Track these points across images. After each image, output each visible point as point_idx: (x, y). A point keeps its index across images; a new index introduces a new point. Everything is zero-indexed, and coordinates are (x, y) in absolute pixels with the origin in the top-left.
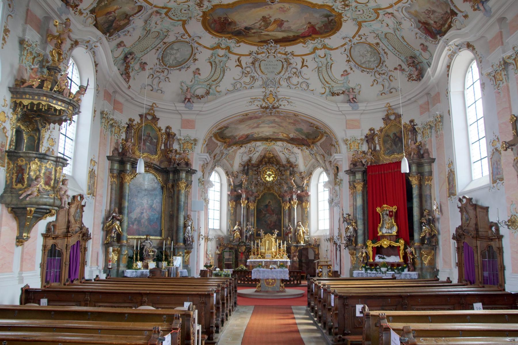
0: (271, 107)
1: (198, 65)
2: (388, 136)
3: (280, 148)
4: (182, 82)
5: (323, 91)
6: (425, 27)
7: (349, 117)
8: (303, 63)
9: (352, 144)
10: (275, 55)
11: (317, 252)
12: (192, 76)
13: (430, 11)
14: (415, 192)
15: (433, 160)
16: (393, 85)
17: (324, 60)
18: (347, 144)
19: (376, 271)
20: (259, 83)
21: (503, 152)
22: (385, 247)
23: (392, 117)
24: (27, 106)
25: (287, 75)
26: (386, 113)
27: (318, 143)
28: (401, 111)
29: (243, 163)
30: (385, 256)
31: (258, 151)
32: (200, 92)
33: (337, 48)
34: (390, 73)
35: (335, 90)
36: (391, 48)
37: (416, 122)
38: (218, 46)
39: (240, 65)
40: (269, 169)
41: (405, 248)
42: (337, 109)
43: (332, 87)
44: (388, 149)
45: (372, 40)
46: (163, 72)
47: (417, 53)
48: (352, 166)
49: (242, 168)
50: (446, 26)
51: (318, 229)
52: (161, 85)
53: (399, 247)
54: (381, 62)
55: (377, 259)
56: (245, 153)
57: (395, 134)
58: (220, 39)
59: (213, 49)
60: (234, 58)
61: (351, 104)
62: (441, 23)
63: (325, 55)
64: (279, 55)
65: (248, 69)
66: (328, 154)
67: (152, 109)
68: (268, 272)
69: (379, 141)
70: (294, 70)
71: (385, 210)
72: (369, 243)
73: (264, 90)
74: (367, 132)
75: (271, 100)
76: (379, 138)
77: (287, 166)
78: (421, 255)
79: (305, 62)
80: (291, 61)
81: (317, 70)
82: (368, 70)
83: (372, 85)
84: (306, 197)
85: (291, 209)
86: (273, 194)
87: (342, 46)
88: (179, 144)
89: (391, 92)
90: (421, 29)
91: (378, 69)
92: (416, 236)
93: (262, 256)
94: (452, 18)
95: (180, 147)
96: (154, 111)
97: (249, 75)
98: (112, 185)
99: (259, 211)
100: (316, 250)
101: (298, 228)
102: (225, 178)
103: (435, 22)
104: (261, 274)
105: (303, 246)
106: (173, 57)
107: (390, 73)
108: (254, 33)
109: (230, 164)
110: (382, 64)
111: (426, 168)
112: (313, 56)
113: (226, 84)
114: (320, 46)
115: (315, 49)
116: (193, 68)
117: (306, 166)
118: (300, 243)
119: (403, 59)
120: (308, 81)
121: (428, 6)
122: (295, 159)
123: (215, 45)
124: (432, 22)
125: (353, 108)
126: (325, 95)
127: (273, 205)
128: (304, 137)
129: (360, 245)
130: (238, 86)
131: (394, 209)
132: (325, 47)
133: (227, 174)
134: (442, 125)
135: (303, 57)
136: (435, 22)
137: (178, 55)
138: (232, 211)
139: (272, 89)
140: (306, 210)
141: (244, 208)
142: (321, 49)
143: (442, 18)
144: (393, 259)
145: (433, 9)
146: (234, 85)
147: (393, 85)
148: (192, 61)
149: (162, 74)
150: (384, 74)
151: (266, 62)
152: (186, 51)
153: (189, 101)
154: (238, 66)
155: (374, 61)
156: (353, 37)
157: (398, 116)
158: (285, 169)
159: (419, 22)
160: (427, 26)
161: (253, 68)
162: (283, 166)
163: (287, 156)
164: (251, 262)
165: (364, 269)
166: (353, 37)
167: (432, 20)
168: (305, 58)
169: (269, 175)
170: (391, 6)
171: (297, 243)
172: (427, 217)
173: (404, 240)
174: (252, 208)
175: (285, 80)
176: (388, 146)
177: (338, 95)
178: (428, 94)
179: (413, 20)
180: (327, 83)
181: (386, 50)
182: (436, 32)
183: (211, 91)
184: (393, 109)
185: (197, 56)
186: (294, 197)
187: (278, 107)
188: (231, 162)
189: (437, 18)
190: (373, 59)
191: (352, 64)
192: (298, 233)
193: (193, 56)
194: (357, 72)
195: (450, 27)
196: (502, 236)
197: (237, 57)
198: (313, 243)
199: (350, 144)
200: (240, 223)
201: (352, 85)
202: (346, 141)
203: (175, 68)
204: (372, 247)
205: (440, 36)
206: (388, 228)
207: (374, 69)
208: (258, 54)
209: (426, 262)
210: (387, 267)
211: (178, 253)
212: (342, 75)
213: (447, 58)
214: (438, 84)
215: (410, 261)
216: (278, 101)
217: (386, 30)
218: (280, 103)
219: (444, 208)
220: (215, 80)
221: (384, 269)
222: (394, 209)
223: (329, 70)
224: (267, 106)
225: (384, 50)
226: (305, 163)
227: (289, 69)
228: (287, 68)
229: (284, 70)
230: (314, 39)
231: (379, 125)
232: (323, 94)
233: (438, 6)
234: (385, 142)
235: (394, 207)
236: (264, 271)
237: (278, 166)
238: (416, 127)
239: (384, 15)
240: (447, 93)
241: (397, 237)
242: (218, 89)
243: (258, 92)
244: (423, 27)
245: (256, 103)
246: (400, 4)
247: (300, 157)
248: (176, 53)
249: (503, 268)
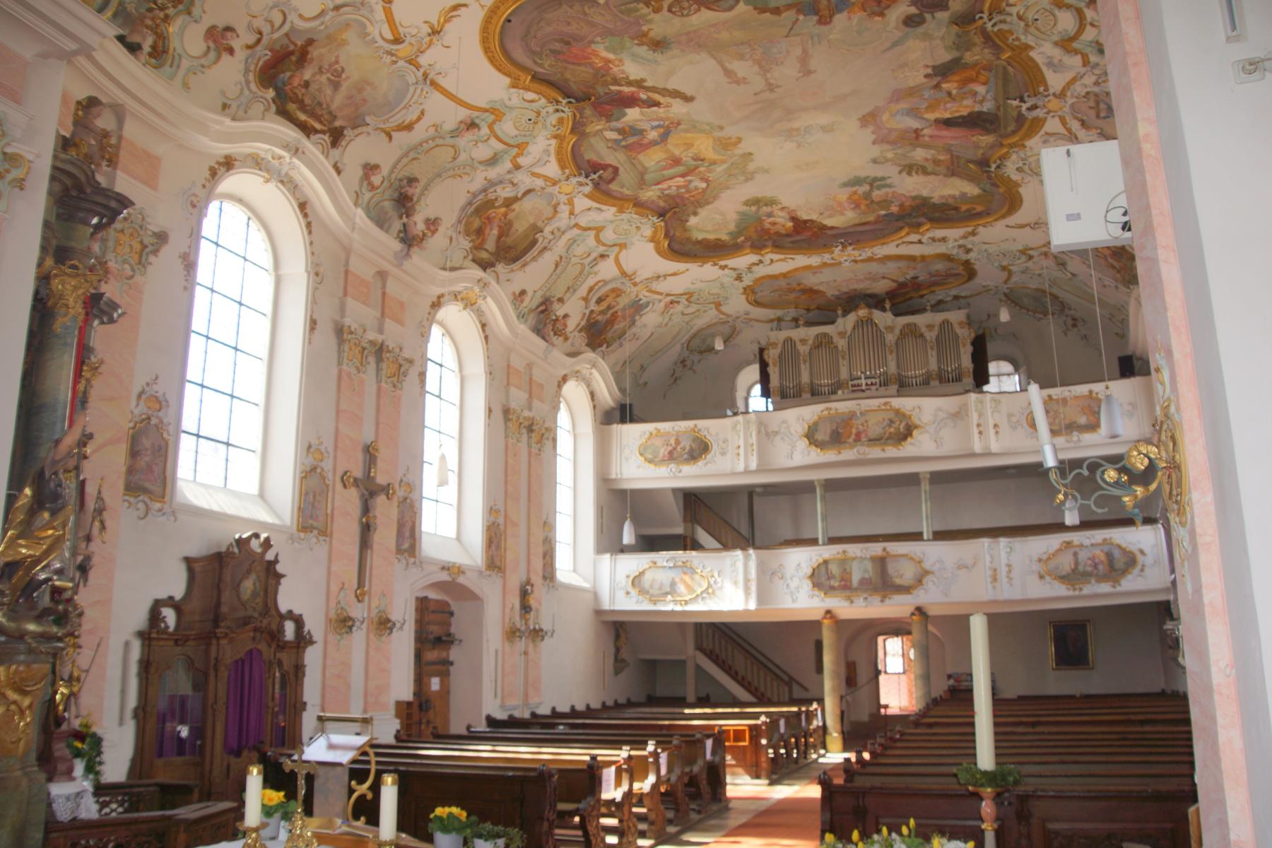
6: (292, 53)
13: (339, 76)
62: (307, 101)
90: (286, 41)
94: (323, 132)
103: (307, 84)
121: (353, 74)
124: (307, 76)
143: (320, 104)
145: (345, 86)
159: (310, 42)
167: (314, 75)
182: (280, 85)
189: (319, 90)
195: (307, 130)
233: (350, 97)
244: (292, 47)
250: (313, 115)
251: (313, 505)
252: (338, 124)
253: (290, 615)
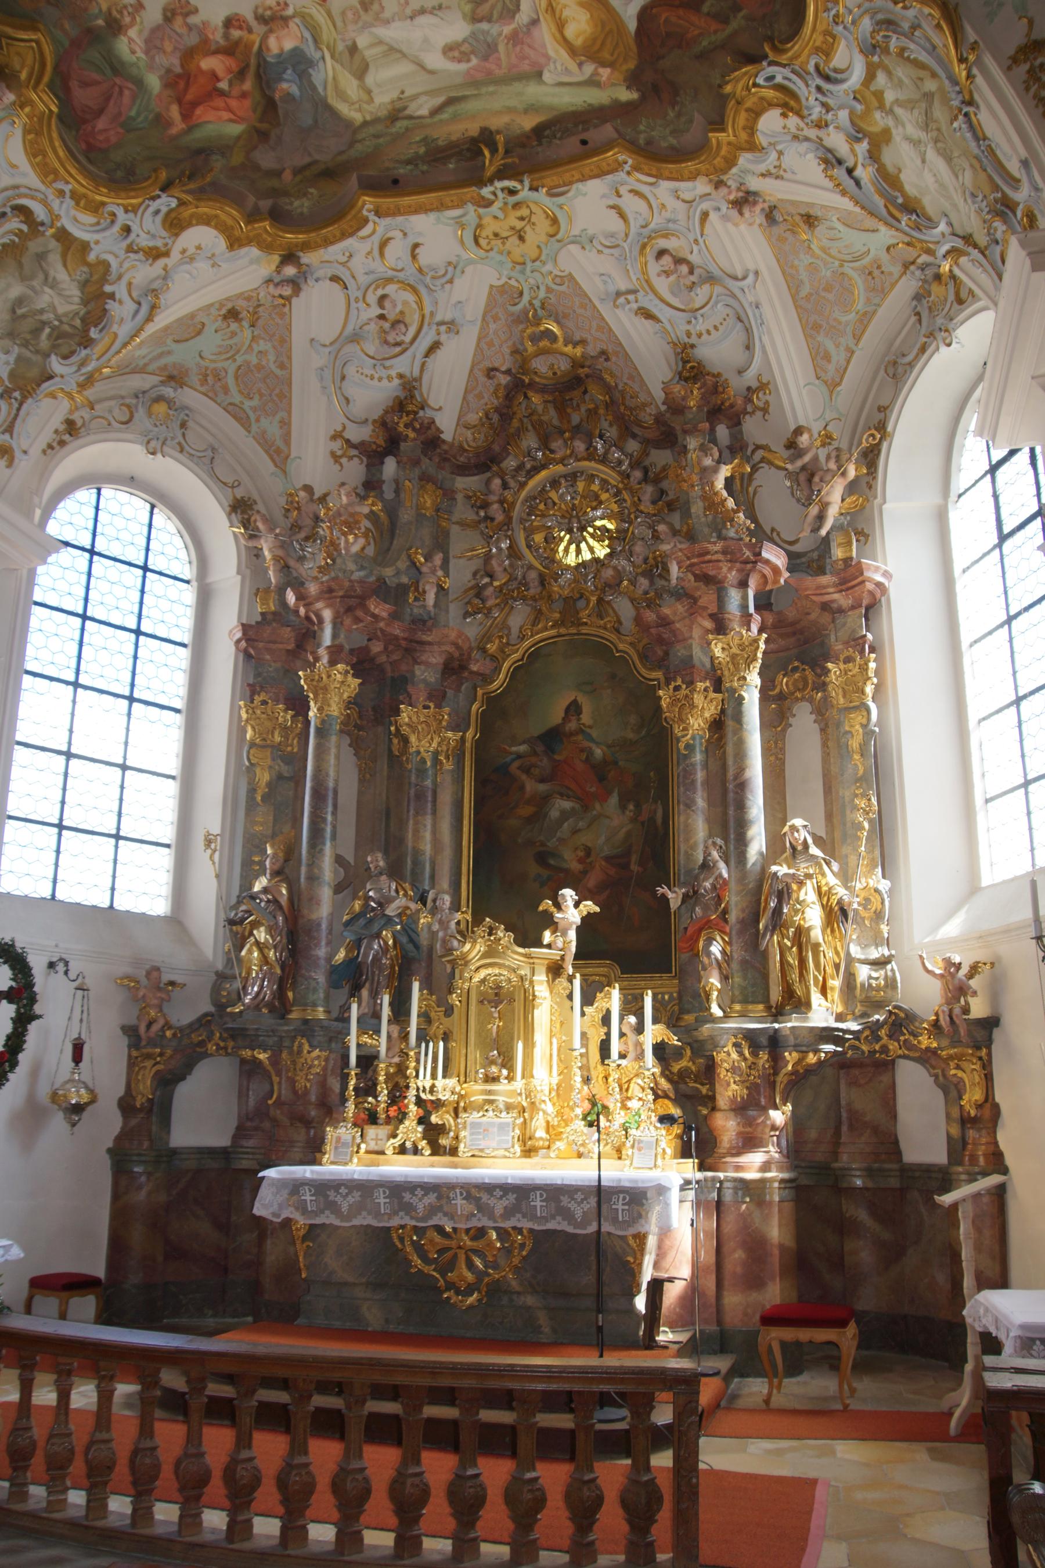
3: (606, 264)
11: (973, 1095)
29: (357, 434)
31: (452, 326)
49: (355, 470)
51: (973, 888)
56: (355, 338)
84: (855, 620)
85: (724, 726)
86: (601, 651)
93: (433, 1133)
99: (493, 783)
100: (969, 1075)
101: (781, 870)
102: (225, 538)
105: (827, 1035)
109: (264, 442)
117: (832, 386)
118: (803, 1005)
122: (737, 335)
127: (601, 725)
133: (241, 509)
138: (264, 777)
140: (854, 723)
141: (321, 732)
163: (679, 326)
164: (296, 1186)
171: (777, 1013)
174: (424, 745)
188: (272, 427)
192: (777, 921)
198: (924, 996)
200: (290, 853)
226: (819, 357)
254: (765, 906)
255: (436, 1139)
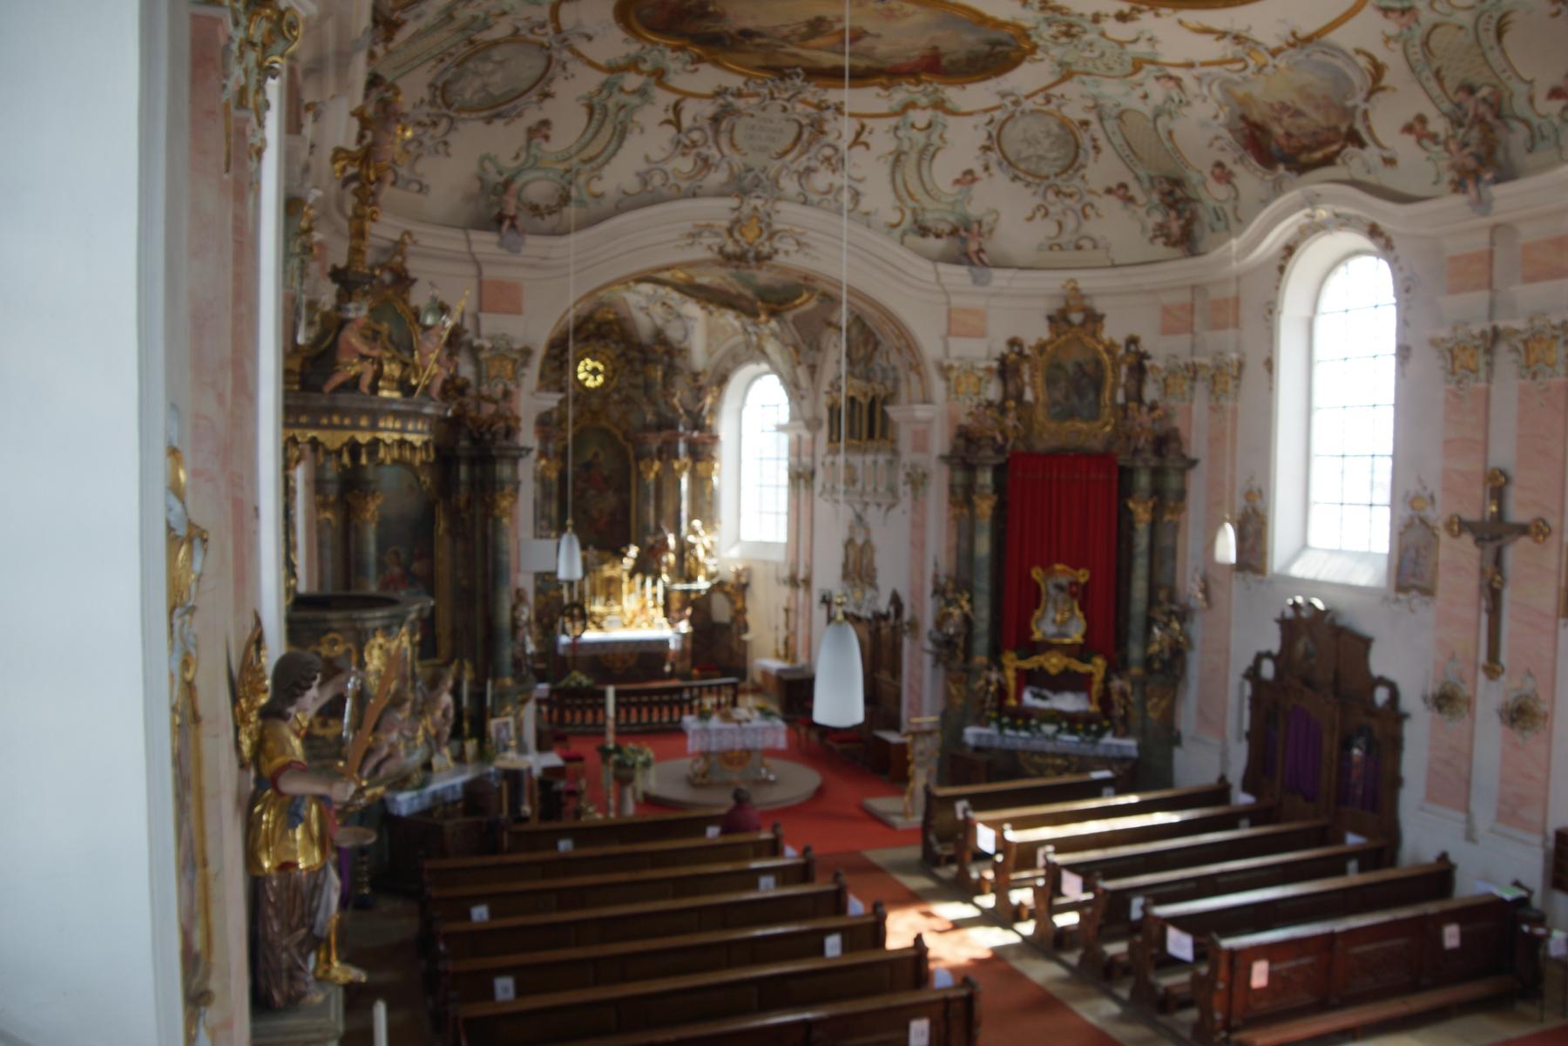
0: (751, 255)
1: (549, 110)
2: (1059, 366)
4: (486, 158)
5: (895, 217)
7: (957, 301)
8: (859, 134)
9: (963, 379)
10: (789, 105)
11: (739, 605)
12: (521, 139)
14: (1142, 541)
15: (1193, 463)
16: (1090, 227)
17: (920, 138)
18: (948, 379)
19: (1027, 728)
20: (717, 178)
21: (1444, 537)
22: (1053, 671)
23: (1076, 318)
24: (339, 453)
25: (804, 162)
26: (1061, 304)
27: (789, 316)
28: (1099, 305)
30: (1046, 693)
32: (538, 189)
33: (970, 114)
34: (1088, 198)
35: (929, 219)
36: (1118, 140)
37: (1145, 345)
38: (633, 65)
39: (677, 123)
40: (595, 352)
41: (1107, 680)
42: (932, 278)
43: (923, 209)
44: (1055, 403)
45: (1074, 112)
46: (435, 124)
47: (1194, 178)
48: (961, 442)
50: (1318, 155)
52: (421, 167)
53: (1090, 675)
54: (1073, 164)
55: (1028, 699)
57: (1079, 365)
58: (648, 46)
59: (614, 69)
60: (664, 98)
61: (975, 270)
62: (1306, 141)
63: (930, 125)
64: (800, 107)
65: (696, 136)
66: (811, 346)
67: (401, 253)
68: (732, 731)
69: (1032, 376)
70: (828, 152)
71: (1055, 578)
72: (1011, 661)
73: (734, 202)
74: (1001, 347)
75: (751, 234)
76: (1034, 369)
77: (655, 352)
78: (1145, 697)
79: (865, 134)
80: (827, 127)
81: (891, 158)
82: (1030, 179)
83: (1030, 219)
87: (986, 111)
88: (477, 362)
89: (1079, 248)
91: (1059, 182)
92: (1135, 652)
94: (1343, 147)
95: (479, 374)
96: (404, 259)
97: (694, 151)
98: (320, 531)
101: (691, 539)
103: (1289, 135)
104: (714, 739)
106: (477, 83)
107: (1088, 198)
108: (759, 45)
110: (1077, 170)
111: (1173, 482)
112: (893, 121)
113: (619, 175)
114: (924, 101)
115: (911, 105)
116: (532, 117)
119: (1142, 173)
120: (860, 187)
121: (1289, 97)
123: (622, 62)
125: (976, 281)
126: (898, 232)
128: (748, 293)
129: (980, 659)
130: (657, 180)
131: (1083, 576)
132: (939, 105)
134: (1237, 387)
135: (866, 121)
136: (1289, 135)
137: (498, 77)
139: (759, 203)
142: (924, 108)
143: (1314, 134)
144: (1068, 702)
145: (1300, 105)
146: (644, 179)
147: (1090, 227)
148: (534, 99)
149: (431, 131)
150: (1071, 196)
151: (753, 121)
152: (526, 67)
153: (513, 226)
154: (668, 122)
155: (1055, 159)
156: (1027, 97)
157: (1094, 319)
158: (645, 359)
159: (1243, 118)
160: (1258, 133)
161: (710, 133)
162: (641, 348)
163: (659, 322)
165: (994, 725)
166: (1027, 97)
168: (869, 122)
169: (595, 372)
170: (1190, 65)
172: (1166, 607)
173: (1108, 658)
175: (795, 177)
176: (1058, 395)
177: (938, 236)
178: (1193, 287)
179: (1227, 109)
180: (911, 196)
181: (1102, 142)
183: (574, 193)
184: (1083, 297)
185: (554, 88)
186: (682, 447)
187: (769, 257)
190: (1053, 155)
191: (994, 156)
193: (541, 87)
194: (1001, 178)
195: (1328, 161)
196: (1405, 716)
197: (672, 98)
198: (731, 578)
199: (958, 378)
201: (975, 210)
202: (945, 371)
203: (474, 115)
204: (1018, 670)
205: (1288, 169)
206: (1059, 623)
207: (1047, 177)
208: (739, 94)
209: (1153, 715)
210: (1058, 723)
211: (503, 707)
212: (957, 182)
213: (1294, 229)
214: (1238, 278)
215: (1119, 712)
216: (771, 236)
217: (1138, 105)
218: (777, 244)
219: (1217, 593)
220: (591, 159)
221: (1049, 729)
222: (1083, 576)
223: (925, 164)
224: (738, 250)
225: (1094, 140)
226: (709, 345)
227: (814, 149)
228: (810, 144)
229: (798, 148)
230: (919, 82)
231: (1035, 332)
232: (895, 226)
234: (1051, 382)
235: (1081, 572)
236: (719, 732)
237: (622, 346)
238: (1147, 363)
239: (1158, 78)
240: (1271, 312)
241: (1083, 652)
242: (597, 187)
243: (718, 210)
245: (708, 240)
246: (1214, 69)
247: (701, 332)
248: (492, 73)
249: (1396, 782)
250: (1322, 145)
251: (1416, 563)
252: (1344, 128)
253: (1382, 681)
254: (684, 549)
255: (600, 627)
